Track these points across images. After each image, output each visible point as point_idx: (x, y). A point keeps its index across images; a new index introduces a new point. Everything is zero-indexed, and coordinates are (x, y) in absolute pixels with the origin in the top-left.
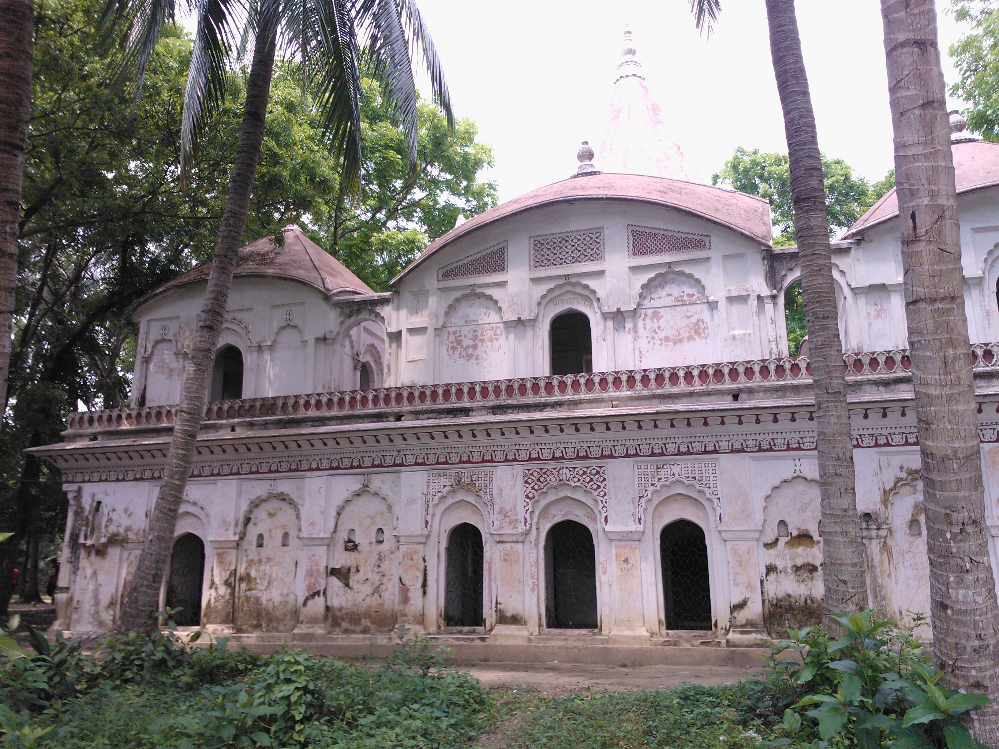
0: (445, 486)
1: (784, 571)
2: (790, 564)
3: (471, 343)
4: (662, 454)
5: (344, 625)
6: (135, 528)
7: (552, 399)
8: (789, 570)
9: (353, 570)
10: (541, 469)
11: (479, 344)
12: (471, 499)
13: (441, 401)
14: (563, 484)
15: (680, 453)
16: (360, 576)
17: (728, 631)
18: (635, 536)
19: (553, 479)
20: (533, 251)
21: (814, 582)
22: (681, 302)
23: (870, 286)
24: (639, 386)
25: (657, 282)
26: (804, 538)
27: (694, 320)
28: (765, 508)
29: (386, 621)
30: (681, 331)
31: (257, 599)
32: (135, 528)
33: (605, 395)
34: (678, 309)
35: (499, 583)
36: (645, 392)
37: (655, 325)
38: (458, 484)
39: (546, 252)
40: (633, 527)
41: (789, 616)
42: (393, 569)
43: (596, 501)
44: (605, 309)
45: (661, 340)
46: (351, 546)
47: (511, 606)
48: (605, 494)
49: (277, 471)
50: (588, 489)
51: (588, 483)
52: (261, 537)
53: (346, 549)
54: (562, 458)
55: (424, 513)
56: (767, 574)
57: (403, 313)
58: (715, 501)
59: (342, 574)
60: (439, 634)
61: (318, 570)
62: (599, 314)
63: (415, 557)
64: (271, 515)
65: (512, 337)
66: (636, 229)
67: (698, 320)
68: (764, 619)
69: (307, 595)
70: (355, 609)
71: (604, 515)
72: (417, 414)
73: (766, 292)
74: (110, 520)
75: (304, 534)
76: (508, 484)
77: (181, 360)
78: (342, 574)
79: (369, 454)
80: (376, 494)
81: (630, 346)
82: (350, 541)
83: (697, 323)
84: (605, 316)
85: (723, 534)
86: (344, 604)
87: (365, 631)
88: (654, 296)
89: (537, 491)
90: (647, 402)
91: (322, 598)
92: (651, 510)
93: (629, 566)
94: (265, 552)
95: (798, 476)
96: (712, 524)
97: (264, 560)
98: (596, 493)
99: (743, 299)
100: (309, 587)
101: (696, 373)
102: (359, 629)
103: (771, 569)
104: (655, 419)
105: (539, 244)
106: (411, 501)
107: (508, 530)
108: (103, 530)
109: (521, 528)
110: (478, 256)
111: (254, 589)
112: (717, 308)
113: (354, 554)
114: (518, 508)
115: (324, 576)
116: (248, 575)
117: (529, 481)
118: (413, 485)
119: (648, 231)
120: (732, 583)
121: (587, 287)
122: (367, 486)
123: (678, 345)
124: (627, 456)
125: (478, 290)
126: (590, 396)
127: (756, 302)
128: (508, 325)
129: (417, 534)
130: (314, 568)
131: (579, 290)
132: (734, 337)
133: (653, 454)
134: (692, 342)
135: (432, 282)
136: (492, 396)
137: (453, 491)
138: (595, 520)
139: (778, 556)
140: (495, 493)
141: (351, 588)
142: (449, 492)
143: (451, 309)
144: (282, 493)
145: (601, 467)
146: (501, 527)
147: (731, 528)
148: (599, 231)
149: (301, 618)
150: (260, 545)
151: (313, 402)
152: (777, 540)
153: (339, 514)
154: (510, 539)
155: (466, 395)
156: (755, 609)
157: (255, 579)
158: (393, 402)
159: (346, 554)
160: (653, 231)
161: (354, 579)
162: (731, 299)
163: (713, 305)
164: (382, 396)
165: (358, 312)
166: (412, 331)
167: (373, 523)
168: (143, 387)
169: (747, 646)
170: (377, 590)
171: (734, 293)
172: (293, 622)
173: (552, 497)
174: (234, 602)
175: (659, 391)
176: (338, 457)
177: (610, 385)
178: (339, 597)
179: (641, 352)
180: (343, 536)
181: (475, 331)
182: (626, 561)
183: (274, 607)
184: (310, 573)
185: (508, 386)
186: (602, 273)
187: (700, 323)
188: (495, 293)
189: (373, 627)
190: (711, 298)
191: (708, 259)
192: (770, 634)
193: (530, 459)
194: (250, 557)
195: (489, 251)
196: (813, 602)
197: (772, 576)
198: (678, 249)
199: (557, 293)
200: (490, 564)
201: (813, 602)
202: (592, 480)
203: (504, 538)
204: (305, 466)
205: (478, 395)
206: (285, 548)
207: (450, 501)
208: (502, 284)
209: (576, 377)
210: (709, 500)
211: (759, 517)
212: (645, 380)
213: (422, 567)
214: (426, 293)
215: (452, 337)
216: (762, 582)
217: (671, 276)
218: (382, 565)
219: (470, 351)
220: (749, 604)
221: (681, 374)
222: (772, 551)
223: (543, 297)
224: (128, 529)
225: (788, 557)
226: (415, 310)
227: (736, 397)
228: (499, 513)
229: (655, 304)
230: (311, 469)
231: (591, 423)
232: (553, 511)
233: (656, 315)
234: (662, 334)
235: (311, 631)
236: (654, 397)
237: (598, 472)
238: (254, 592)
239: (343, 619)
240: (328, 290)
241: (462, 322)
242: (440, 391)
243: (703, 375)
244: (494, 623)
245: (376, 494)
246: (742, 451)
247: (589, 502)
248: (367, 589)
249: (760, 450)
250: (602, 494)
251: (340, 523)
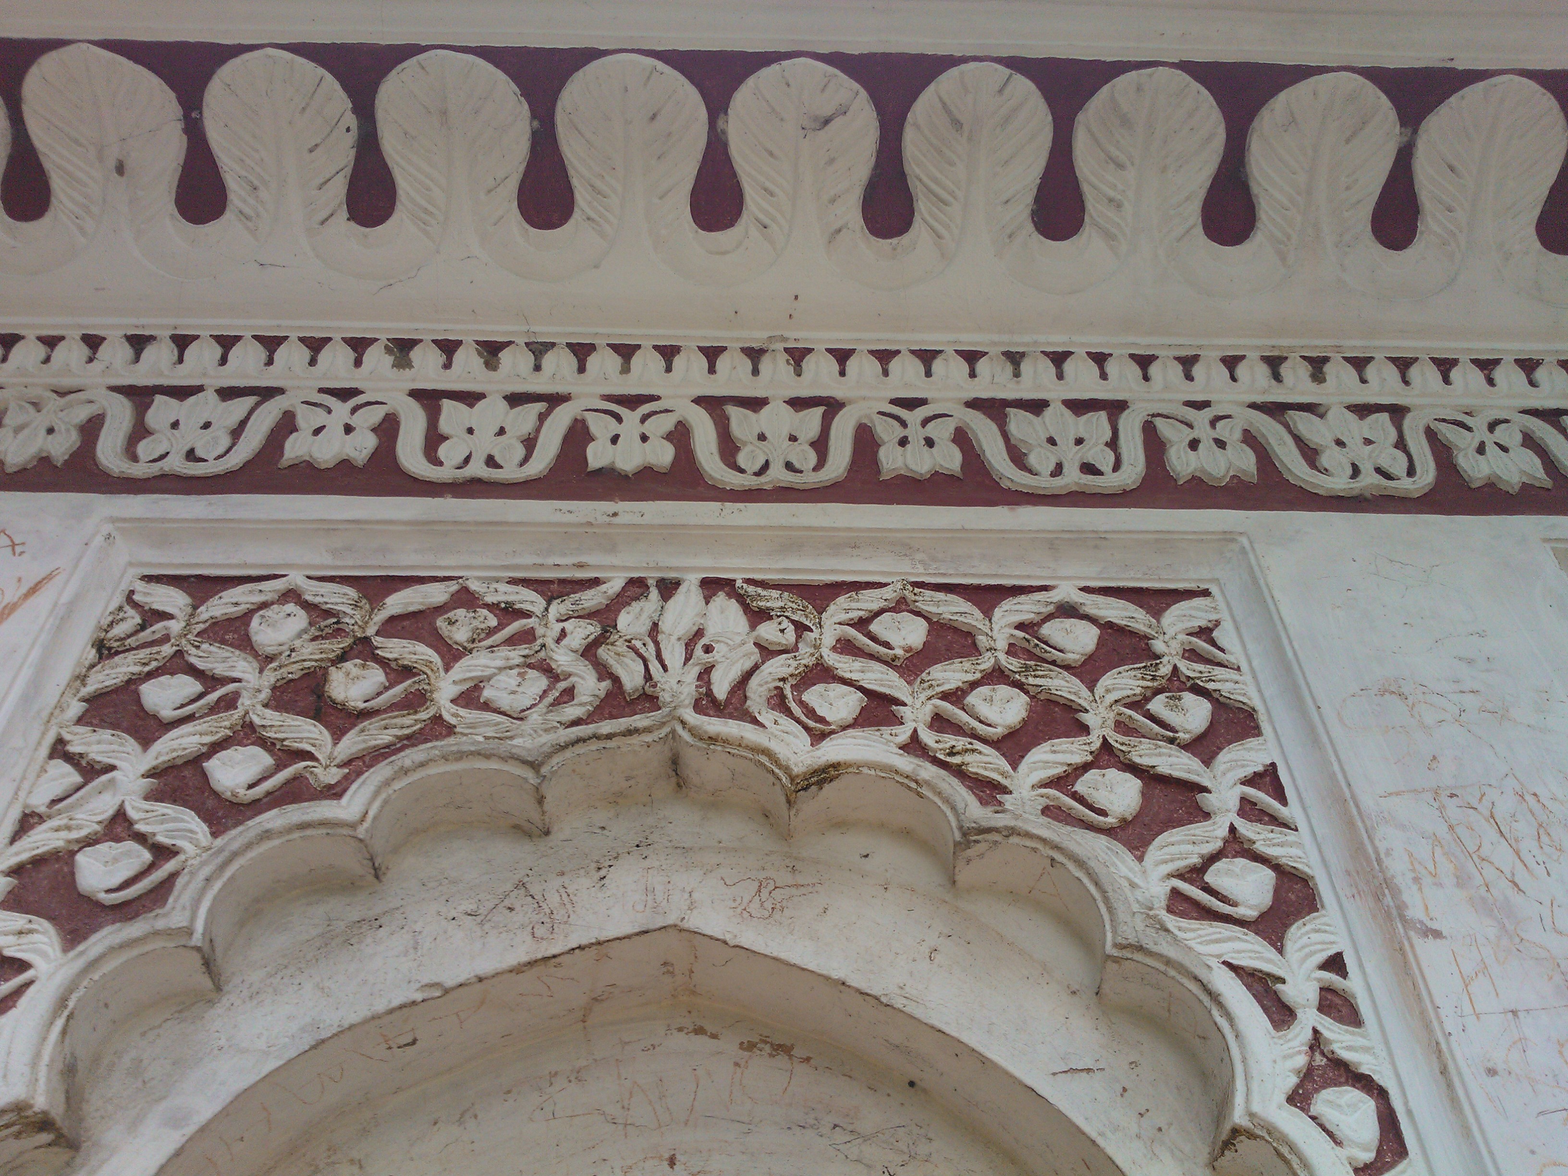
10: (373, 588)
14: (647, 752)
51: (1014, 744)
89: (222, 813)
98: (1144, 879)
117: (164, 695)
173: (441, 941)
202: (1055, 718)
250: (1248, 886)
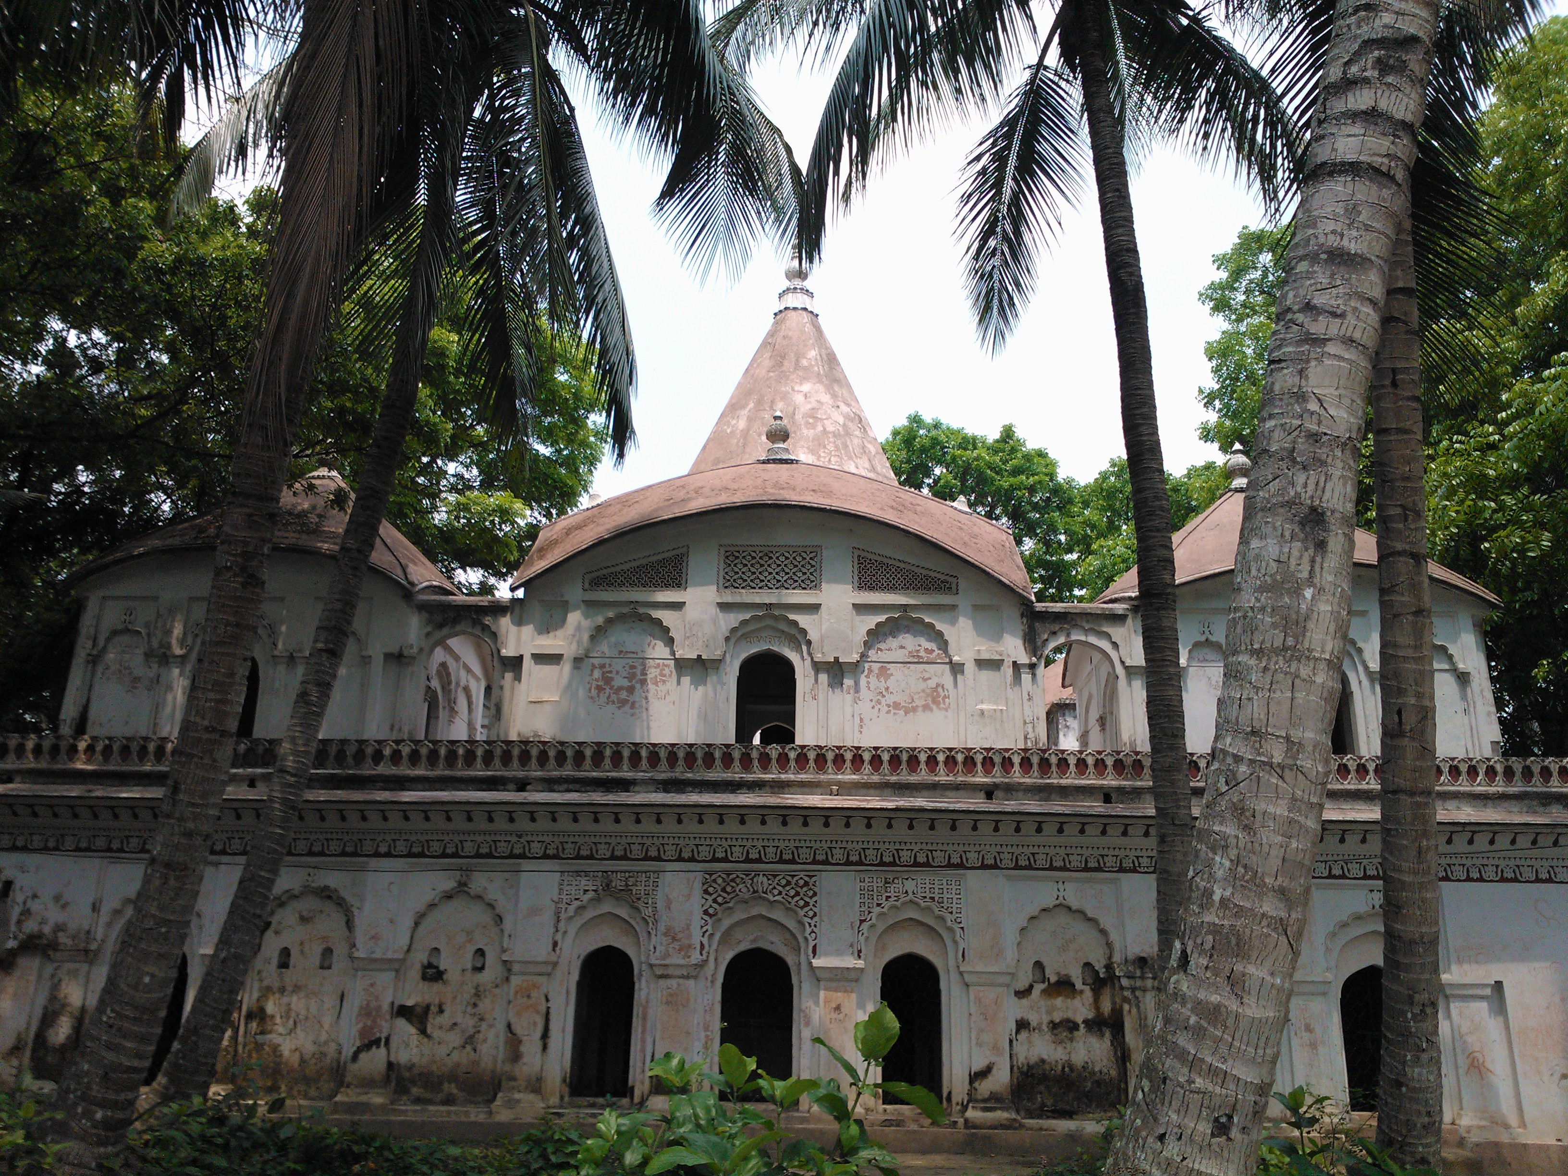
0: (586, 891)
1: (1038, 1028)
2: (1045, 1019)
3: (626, 683)
4: (893, 864)
5: (415, 1091)
6: (72, 926)
7: (750, 777)
8: (1044, 1027)
9: (434, 1009)
11: (638, 686)
12: (623, 912)
13: (587, 767)
14: (757, 896)
15: (916, 864)
16: (445, 1019)
17: (965, 1108)
18: (853, 975)
19: (744, 890)
20: (722, 565)
21: (1075, 1044)
24: (867, 768)
25: (886, 629)
26: (1063, 986)
27: (932, 683)
28: (1019, 944)
29: (484, 1087)
30: (916, 697)
31: (275, 1048)
32: (72, 926)
33: (823, 777)
35: (658, 1035)
36: (876, 778)
37: (882, 685)
38: (607, 890)
39: (739, 569)
40: (851, 962)
41: (1042, 1088)
42: (495, 1009)
43: (801, 923)
44: (818, 657)
46: (433, 974)
47: (668, 1071)
48: (815, 915)
49: (322, 854)
50: (792, 906)
52: (286, 953)
53: (424, 978)
54: (759, 861)
55: (552, 930)
56: (1018, 1032)
57: (528, 630)
58: (958, 931)
59: (416, 1016)
60: (561, 1107)
61: (380, 1007)
62: (808, 662)
63: (534, 994)
64: (304, 920)
65: (686, 680)
66: (863, 554)
67: (938, 685)
68: (1013, 1092)
69: (358, 1044)
70: (434, 1068)
71: (812, 944)
72: (550, 784)
73: (1024, 658)
74: (26, 913)
75: (360, 953)
76: (680, 895)
77: (155, 666)
78: (416, 1016)
79: (472, 837)
80: (479, 897)
81: (848, 710)
82: (430, 965)
84: (818, 667)
85: (966, 976)
86: (416, 1060)
87: (449, 1101)
88: (882, 646)
90: (878, 792)
91: (383, 1051)
92: (873, 939)
93: (841, 1016)
94: (290, 976)
95: (1060, 905)
96: (952, 962)
97: (289, 988)
98: (802, 913)
99: (993, 664)
100: (363, 1033)
101: (941, 758)
102: (439, 1097)
103: (1022, 1025)
104: (890, 816)
105: (731, 557)
106: (534, 911)
107: (676, 959)
108: (13, 928)
109: (696, 957)
110: (644, 562)
111: (270, 1032)
112: (962, 672)
113: (437, 987)
114: (692, 928)
115: (388, 1017)
116: (262, 1010)
117: (711, 890)
118: (539, 888)
119: (879, 559)
120: (974, 1042)
121: (795, 623)
122: (465, 885)
124: (848, 863)
125: (641, 610)
126: (803, 777)
127: (1010, 671)
128: (682, 665)
129: (539, 959)
130: (373, 1004)
131: (782, 626)
132: (982, 712)
133: (882, 864)
134: (928, 713)
135: (575, 592)
136: (664, 764)
137: (597, 900)
138: (797, 950)
139: (1032, 1008)
140: (660, 905)
141: (429, 1037)
142: (592, 900)
143: (598, 633)
144: (326, 888)
145: (811, 877)
146: (667, 955)
147: (978, 969)
148: (815, 552)
149: (348, 1079)
150: (284, 964)
151: (387, 752)
152: (1031, 987)
153: (417, 924)
154: (679, 972)
155: (626, 761)
156: (1001, 1078)
157: (273, 1017)
158: (515, 762)
159: (424, 986)
160: (886, 561)
161: (434, 1023)
162: (981, 663)
163: (957, 669)
164: (498, 752)
165: (455, 621)
166: (540, 658)
167: (470, 941)
168: (84, 701)
169: (992, 1127)
170: (470, 1040)
171: (985, 656)
172: (332, 1085)
174: (236, 1051)
175: (894, 779)
176: (423, 838)
177: (830, 763)
178: (408, 1046)
180: (420, 957)
181: (633, 667)
182: (838, 1008)
183: (303, 1061)
184: (367, 1012)
185: (688, 754)
186: (815, 608)
188: (667, 617)
189: (460, 1095)
190: (956, 659)
191: (954, 607)
192: (1018, 1112)
193: (715, 860)
194: (266, 983)
195: (660, 557)
196: (1072, 1070)
197: (1023, 1035)
198: (916, 589)
199: (751, 627)
200: (645, 1008)
201: (1072, 1070)
202: (797, 894)
203: (670, 971)
204: (368, 847)
205: (644, 762)
206: (326, 972)
207: (590, 914)
208: (678, 606)
209: (783, 748)
210: (951, 930)
211: (1011, 955)
212: (876, 761)
213: (543, 1009)
214: (565, 607)
215: (597, 674)
216: (1011, 1041)
217: (906, 623)
218: (481, 1005)
219: (624, 695)
220: (994, 1071)
221: (923, 757)
222: (1025, 1002)
223: (734, 630)
224: (59, 928)
225: (1043, 1010)
226: (545, 629)
227: (989, 795)
228: (665, 934)
229: (884, 656)
230: (377, 855)
231: (806, 814)
232: (738, 934)
233: (883, 673)
234: (890, 699)
235: (364, 1098)
236: (887, 785)
237: (806, 884)
238: (269, 1036)
239: (414, 1083)
240: (413, 584)
241: (615, 653)
242: (588, 752)
243: (950, 761)
244: (646, 1092)
245: (479, 897)
246: (995, 867)
247: (791, 924)
248: (454, 1039)
249: (1017, 867)
250: (811, 914)
251: (417, 937)
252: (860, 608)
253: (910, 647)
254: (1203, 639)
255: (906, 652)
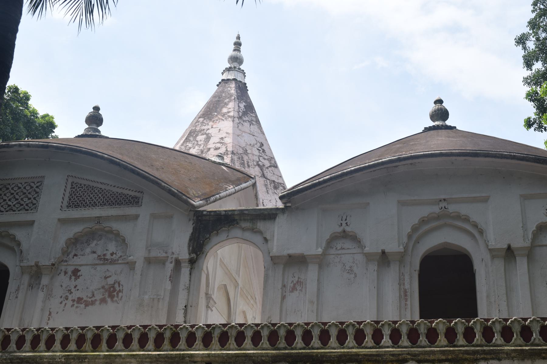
22: (104, 260)
23: (290, 256)
27: (110, 281)
30: (95, 293)
34: (99, 268)
37: (73, 283)
45: (73, 301)
66: (76, 180)
83: (113, 286)
112: (134, 269)
119: (87, 183)
123: (90, 308)
179: (50, 314)
186: (31, 223)
187: (116, 285)
234: (76, 295)
252: (63, 222)
253: (99, 253)
254: (340, 229)
255: (95, 256)
